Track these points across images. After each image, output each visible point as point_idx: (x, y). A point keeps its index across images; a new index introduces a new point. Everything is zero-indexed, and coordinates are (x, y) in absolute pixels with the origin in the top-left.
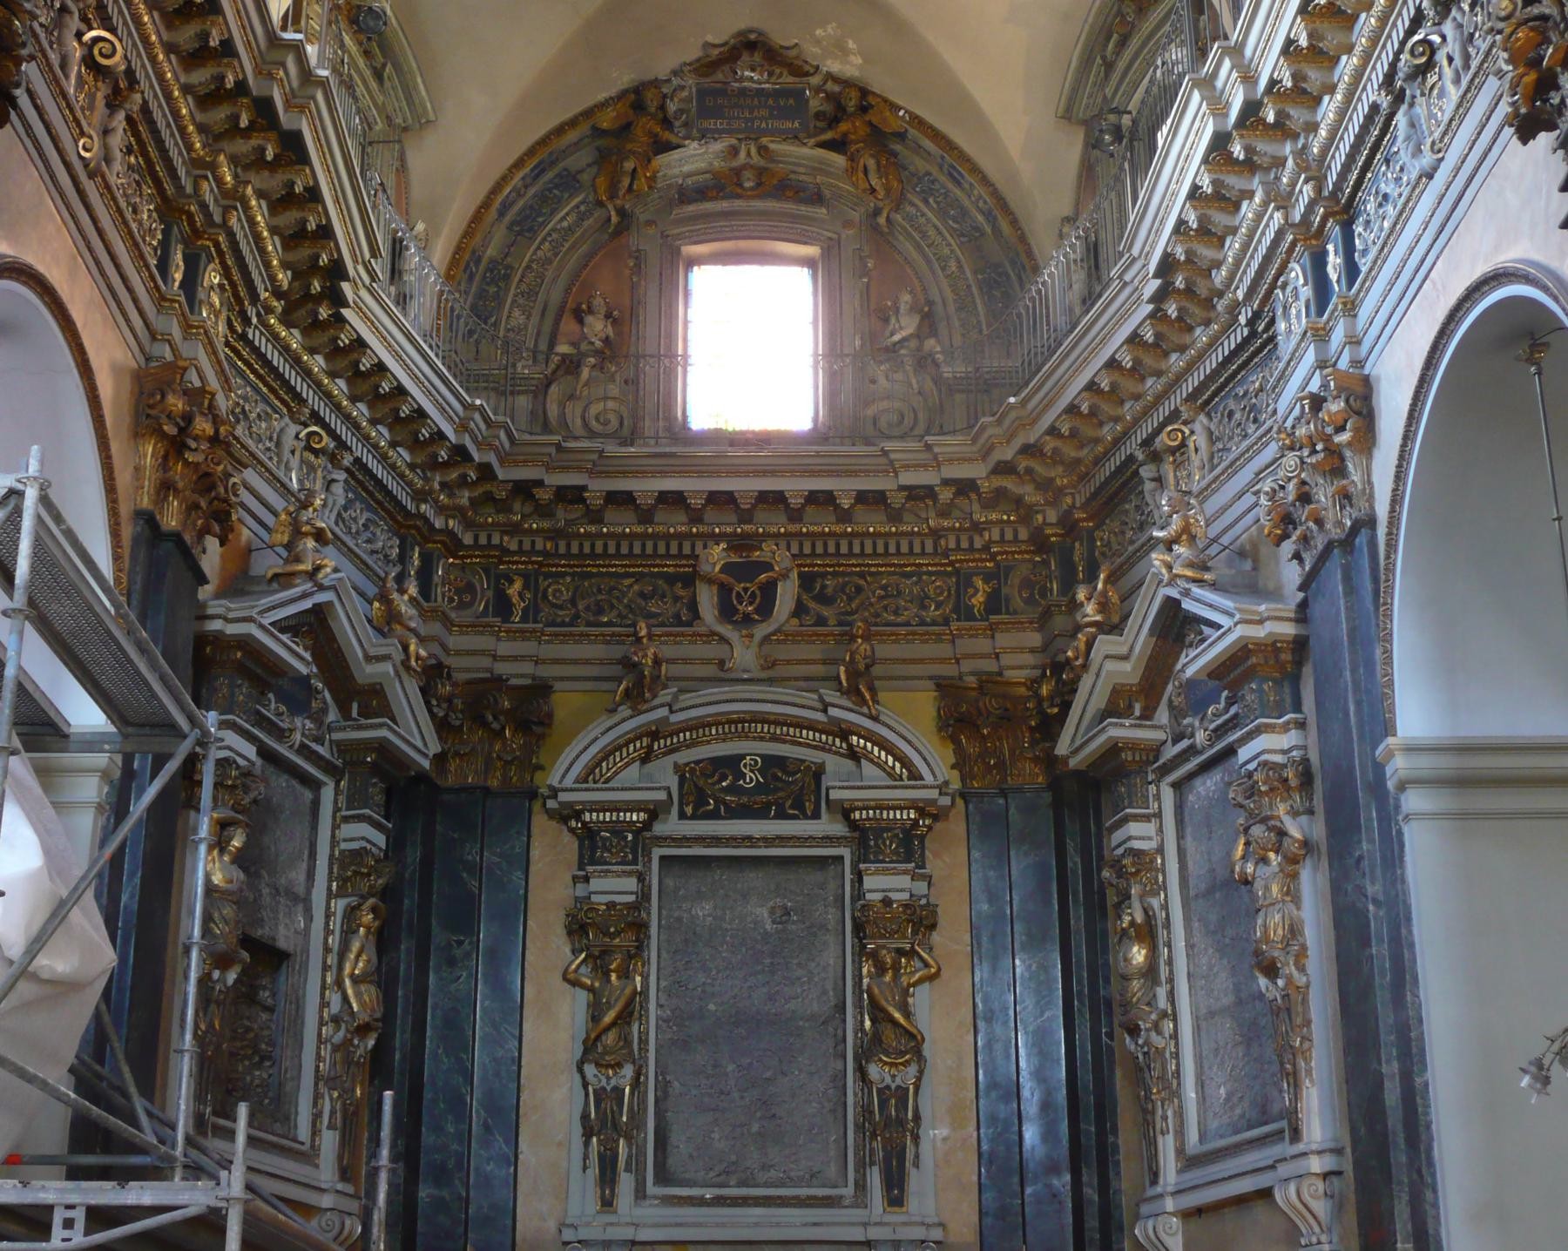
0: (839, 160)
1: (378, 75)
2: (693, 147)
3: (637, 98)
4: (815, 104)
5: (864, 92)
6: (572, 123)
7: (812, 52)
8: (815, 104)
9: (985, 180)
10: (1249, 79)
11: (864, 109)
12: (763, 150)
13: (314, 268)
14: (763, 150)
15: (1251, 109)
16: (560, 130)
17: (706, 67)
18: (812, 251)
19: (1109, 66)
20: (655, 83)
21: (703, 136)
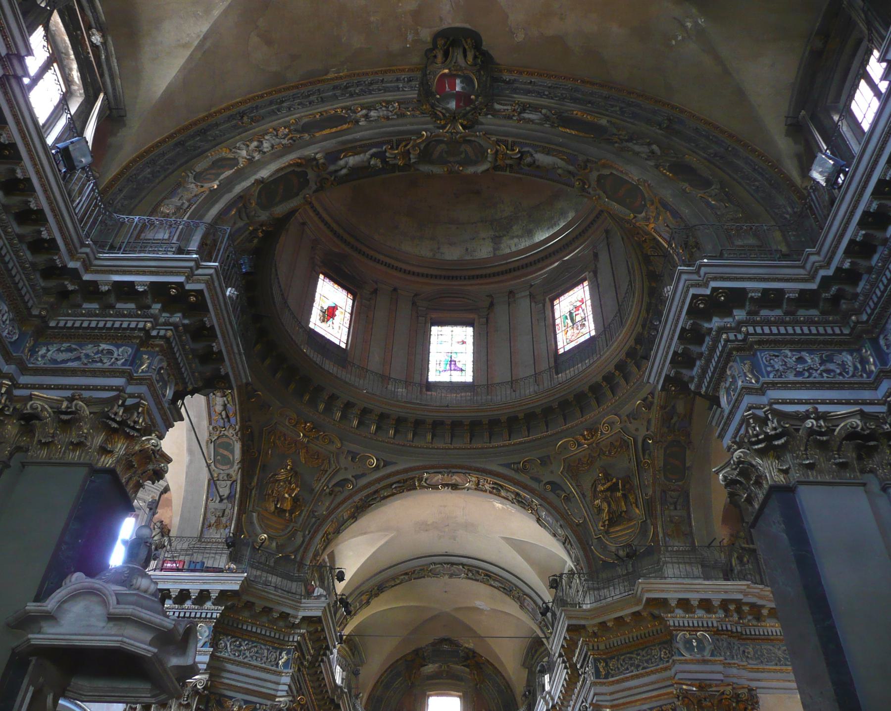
0: (467, 670)
1: (353, 655)
2: (430, 666)
3: (416, 652)
4: (462, 654)
5: (474, 652)
6: (401, 659)
7: (461, 642)
8: (462, 654)
9: (504, 678)
10: (553, 699)
11: (474, 657)
12: (448, 666)
13: (321, 648)
14: (448, 666)
15: (554, 706)
16: (397, 661)
17: (433, 644)
18: (461, 694)
19: (533, 656)
20: (421, 649)
21: (434, 662)
